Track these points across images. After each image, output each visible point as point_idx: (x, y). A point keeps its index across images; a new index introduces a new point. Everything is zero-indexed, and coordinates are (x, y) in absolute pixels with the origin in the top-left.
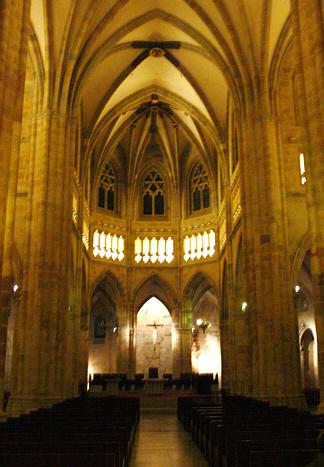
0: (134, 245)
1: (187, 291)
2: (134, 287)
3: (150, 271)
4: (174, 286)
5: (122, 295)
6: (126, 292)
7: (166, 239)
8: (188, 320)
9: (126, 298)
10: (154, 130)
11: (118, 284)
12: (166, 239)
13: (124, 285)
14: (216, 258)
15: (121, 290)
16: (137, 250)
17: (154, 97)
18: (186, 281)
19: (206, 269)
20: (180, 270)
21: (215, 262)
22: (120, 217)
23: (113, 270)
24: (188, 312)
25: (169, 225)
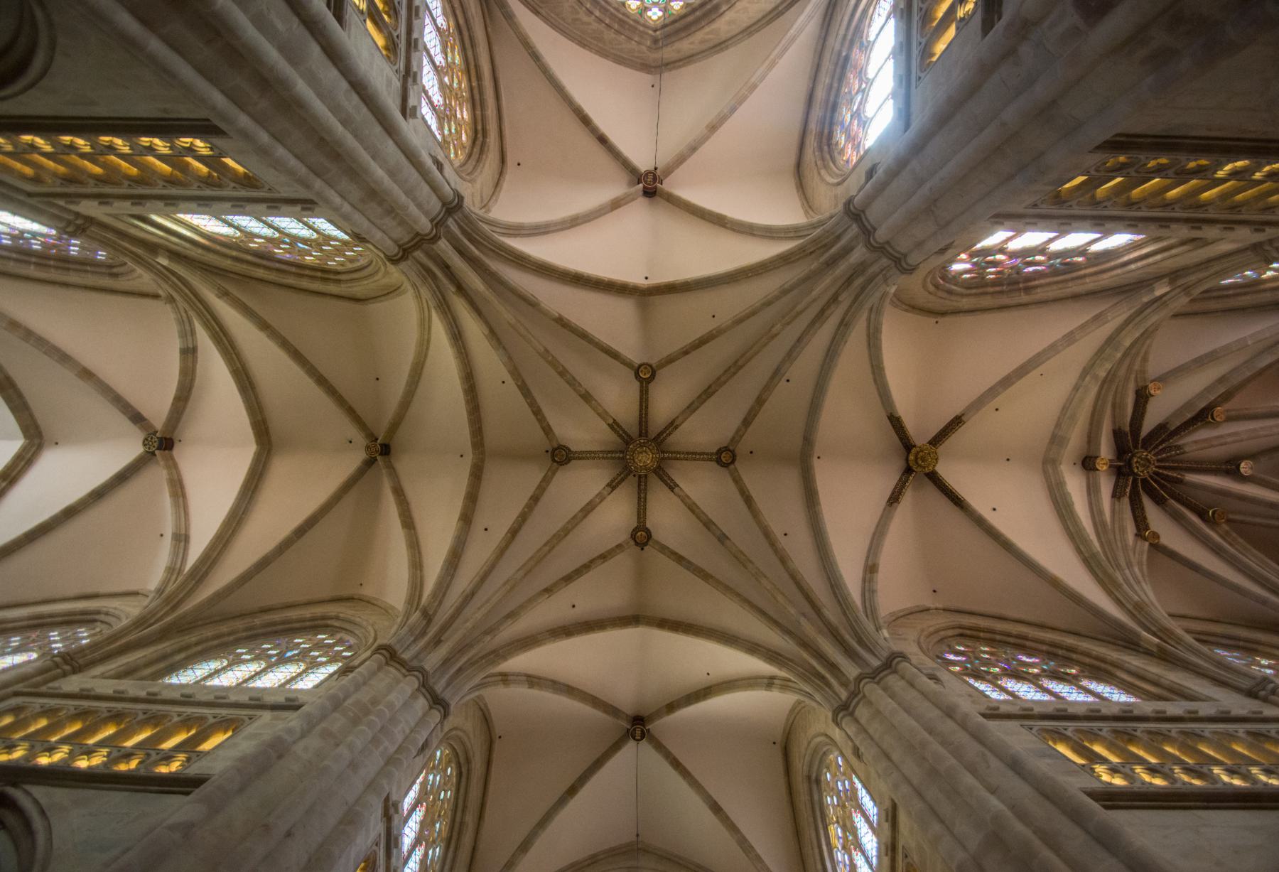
10: (1230, 467)
17: (1088, 463)
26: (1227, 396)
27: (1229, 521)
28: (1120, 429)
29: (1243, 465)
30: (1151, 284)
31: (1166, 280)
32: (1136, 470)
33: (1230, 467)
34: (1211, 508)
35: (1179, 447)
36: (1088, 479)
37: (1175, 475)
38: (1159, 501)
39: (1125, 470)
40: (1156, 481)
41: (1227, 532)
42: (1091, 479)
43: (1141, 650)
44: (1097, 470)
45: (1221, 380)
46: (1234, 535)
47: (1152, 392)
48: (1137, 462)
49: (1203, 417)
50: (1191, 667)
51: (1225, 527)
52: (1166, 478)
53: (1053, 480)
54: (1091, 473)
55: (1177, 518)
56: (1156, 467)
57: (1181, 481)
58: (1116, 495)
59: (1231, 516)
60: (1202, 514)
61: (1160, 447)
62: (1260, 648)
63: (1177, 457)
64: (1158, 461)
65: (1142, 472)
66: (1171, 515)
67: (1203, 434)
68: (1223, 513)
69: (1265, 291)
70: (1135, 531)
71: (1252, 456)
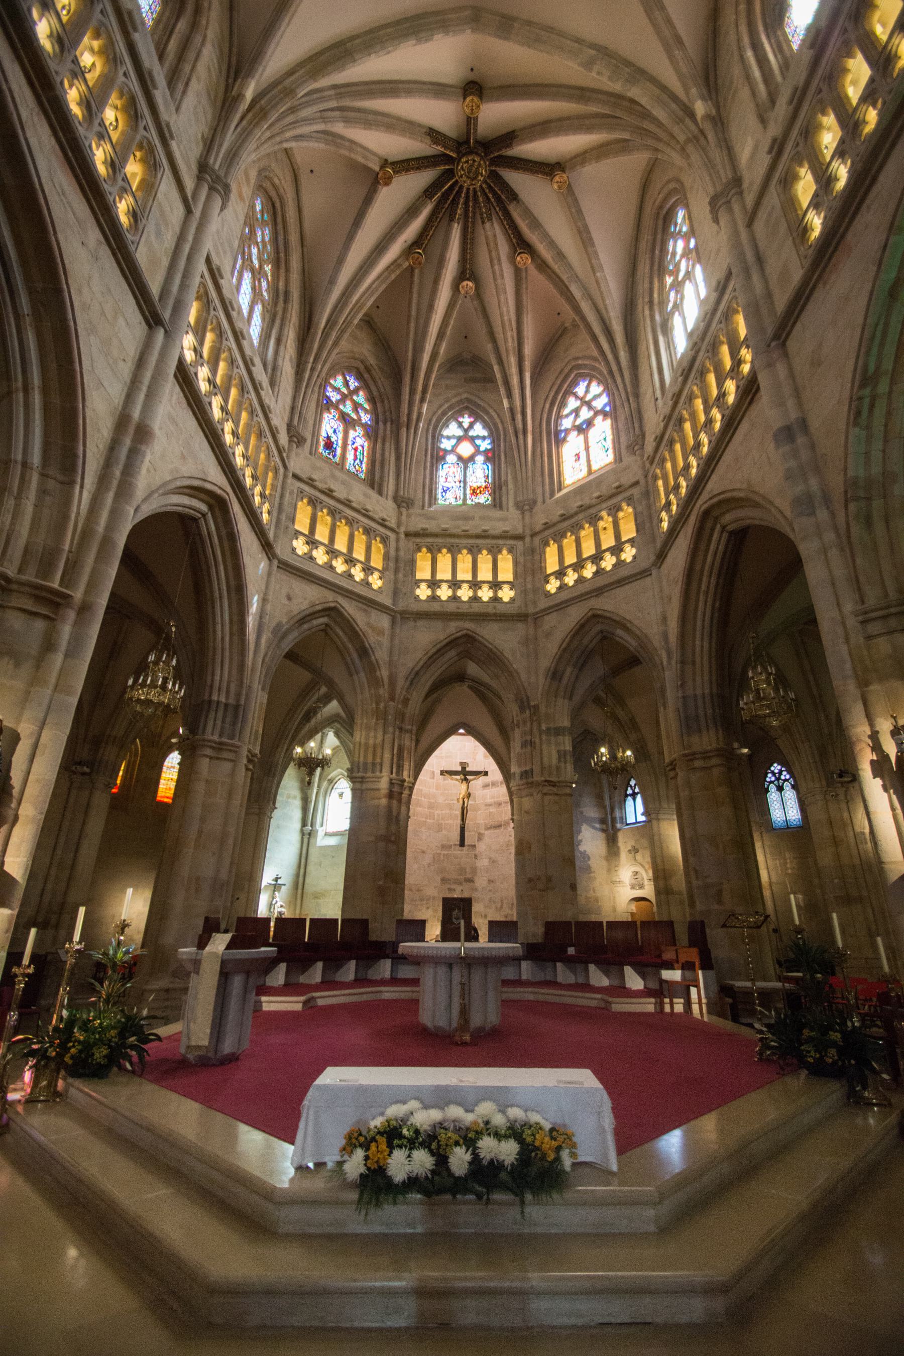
0: (412, 563)
1: (555, 675)
2: (410, 661)
3: (453, 627)
4: (518, 663)
5: (375, 682)
6: (384, 673)
7: (494, 552)
8: (562, 755)
9: (383, 692)
11: (364, 652)
12: (494, 552)
13: (381, 655)
14: (652, 558)
15: (372, 668)
16: (423, 572)
18: (551, 648)
19: (606, 604)
20: (536, 618)
21: (644, 573)
22: (380, 493)
23: (350, 608)
24: (558, 731)
25: (505, 519)
26: (542, 266)
27: (411, 269)
28: (515, 137)
29: (470, 284)
30: (711, 99)
31: (714, 112)
32: (464, 160)
33: (467, 271)
34: (423, 251)
35: (490, 219)
36: (451, 86)
37: (459, 212)
38: (428, 193)
39: (463, 149)
40: (451, 188)
41: (399, 266)
42: (453, 89)
43: (230, 81)
44: (465, 99)
45: (560, 255)
46: (398, 272)
47: (557, 178)
48: (474, 161)
49: (520, 244)
50: (222, 123)
51: (406, 264)
52: (455, 202)
53: (450, 16)
54: (461, 92)
55: (411, 211)
56: (468, 189)
57: (452, 220)
58: (433, 134)
59: (417, 271)
60: (417, 243)
61: (490, 196)
62: (282, 271)
63: (478, 216)
64: (475, 191)
65: (462, 168)
66: (414, 204)
67: (504, 248)
68: (420, 263)
69: (651, 283)
70: (390, 160)
71: (479, 295)
